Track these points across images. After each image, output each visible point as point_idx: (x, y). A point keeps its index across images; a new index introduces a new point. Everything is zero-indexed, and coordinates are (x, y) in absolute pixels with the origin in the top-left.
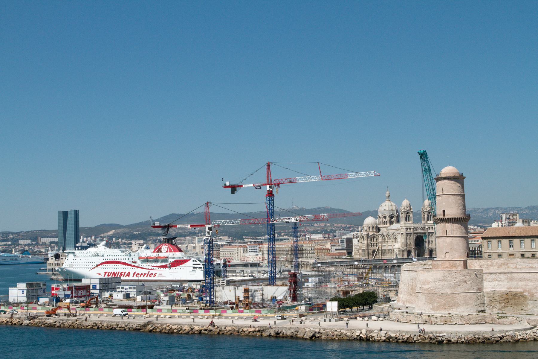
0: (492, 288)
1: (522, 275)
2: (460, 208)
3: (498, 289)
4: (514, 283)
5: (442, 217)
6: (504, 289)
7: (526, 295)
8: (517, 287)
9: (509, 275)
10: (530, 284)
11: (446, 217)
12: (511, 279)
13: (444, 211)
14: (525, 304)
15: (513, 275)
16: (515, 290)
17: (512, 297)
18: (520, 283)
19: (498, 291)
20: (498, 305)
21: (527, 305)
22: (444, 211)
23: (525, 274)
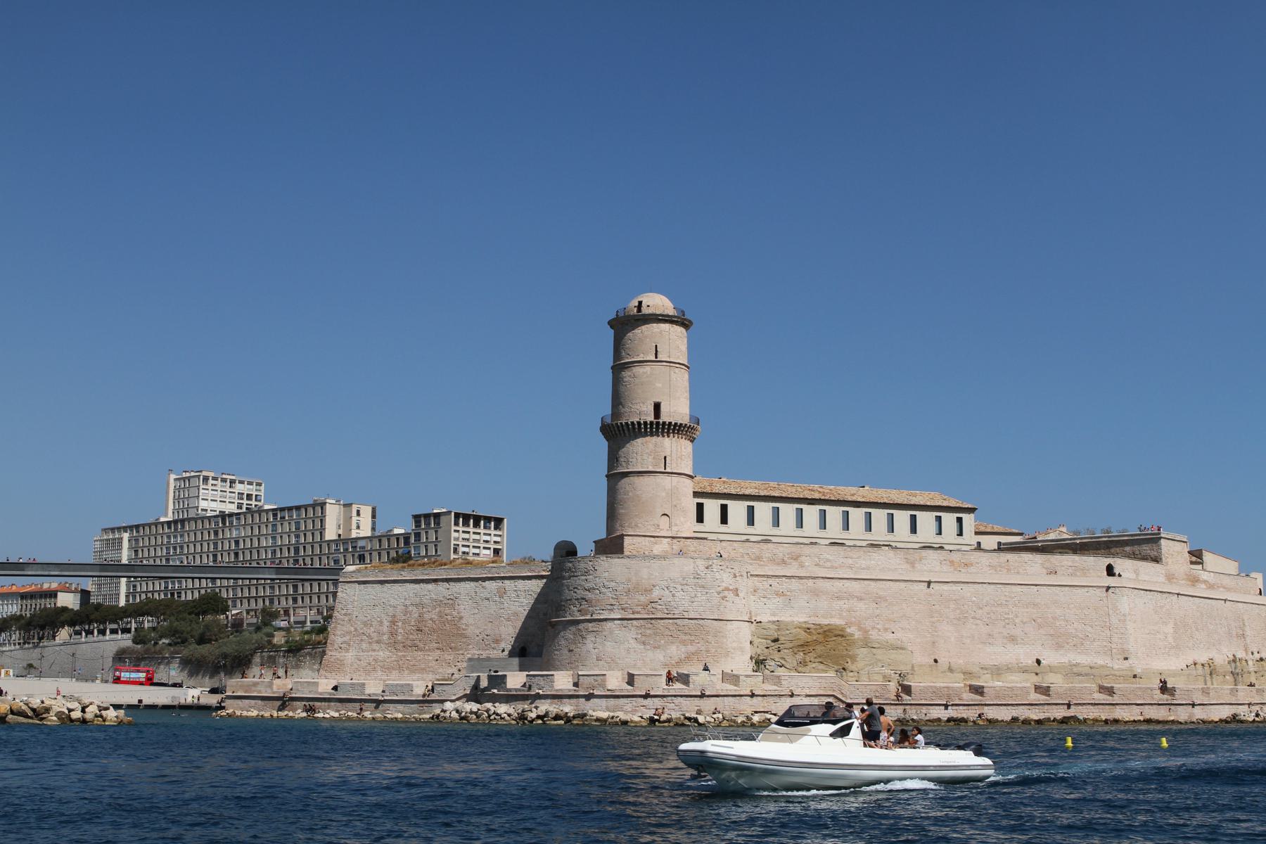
0: (774, 615)
1: (839, 584)
5: (651, 418)
6: (801, 618)
7: (852, 635)
10: (861, 605)
11: (665, 418)
12: (816, 593)
13: (657, 407)
15: (820, 583)
16: (825, 622)
17: (820, 638)
20: (789, 659)
21: (853, 658)
22: (657, 407)
23: (847, 583)
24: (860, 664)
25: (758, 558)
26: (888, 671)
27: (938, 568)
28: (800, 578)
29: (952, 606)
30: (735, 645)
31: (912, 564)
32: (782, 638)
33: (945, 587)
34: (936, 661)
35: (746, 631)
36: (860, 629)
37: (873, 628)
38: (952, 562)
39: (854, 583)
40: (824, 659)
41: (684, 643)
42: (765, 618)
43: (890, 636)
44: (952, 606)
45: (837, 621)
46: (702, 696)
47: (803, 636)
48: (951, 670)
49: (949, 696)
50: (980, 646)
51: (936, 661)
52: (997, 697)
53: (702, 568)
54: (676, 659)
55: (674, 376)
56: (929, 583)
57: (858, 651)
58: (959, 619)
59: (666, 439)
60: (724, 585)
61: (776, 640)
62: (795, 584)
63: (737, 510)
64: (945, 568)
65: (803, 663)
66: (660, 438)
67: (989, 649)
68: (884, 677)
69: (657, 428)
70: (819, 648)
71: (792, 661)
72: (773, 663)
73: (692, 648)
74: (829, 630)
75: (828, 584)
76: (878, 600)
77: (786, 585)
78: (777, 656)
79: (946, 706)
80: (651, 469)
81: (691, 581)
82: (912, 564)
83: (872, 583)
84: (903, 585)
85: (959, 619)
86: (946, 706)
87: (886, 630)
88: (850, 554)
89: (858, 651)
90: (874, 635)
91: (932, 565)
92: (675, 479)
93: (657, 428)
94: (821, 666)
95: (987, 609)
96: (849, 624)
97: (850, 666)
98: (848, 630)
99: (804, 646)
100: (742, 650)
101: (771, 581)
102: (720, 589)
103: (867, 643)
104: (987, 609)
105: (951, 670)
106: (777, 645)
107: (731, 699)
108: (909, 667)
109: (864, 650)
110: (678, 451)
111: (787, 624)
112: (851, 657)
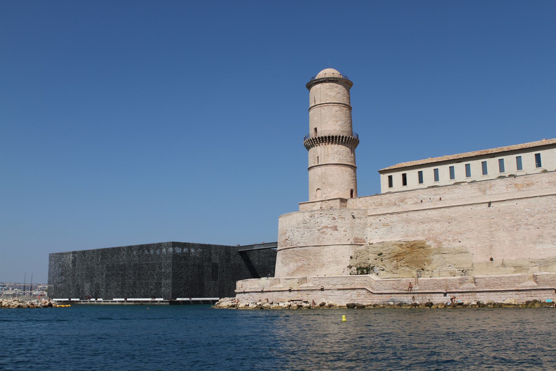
0: (381, 238)
1: (423, 213)
2: (340, 123)
3: (387, 239)
4: (412, 227)
7: (429, 246)
8: (414, 233)
9: (404, 215)
10: (437, 226)
12: (408, 221)
14: (427, 261)
18: (421, 227)
19: (389, 243)
21: (429, 262)
23: (429, 212)
24: (434, 265)
25: (381, 205)
26: (452, 269)
27: (505, 191)
28: (398, 213)
29: (508, 218)
30: (330, 260)
31: (484, 192)
32: (384, 253)
33: (503, 204)
34: (492, 259)
35: (349, 251)
36: (436, 241)
37: (445, 240)
38: (516, 185)
39: (434, 211)
40: (409, 264)
41: (296, 261)
42: (374, 241)
43: (456, 245)
44: (508, 218)
45: (420, 238)
46: (262, 292)
47: (398, 249)
48: (503, 265)
49: (447, 287)
50: (531, 245)
51: (492, 259)
52: (486, 286)
53: (307, 217)
54: (292, 271)
55: (323, 111)
56: (490, 203)
57: (432, 257)
58: (513, 227)
59: (319, 147)
60: (323, 225)
61: (380, 254)
62: (395, 218)
63: (412, 175)
64: (510, 190)
65: (397, 267)
66: (316, 147)
67: (539, 247)
68: (451, 273)
69: (333, 140)
70: (408, 257)
71: (389, 266)
72: (378, 269)
73: (300, 264)
74: (414, 245)
75: (416, 214)
76: (450, 221)
77: (389, 218)
78: (380, 264)
79: (445, 294)
80: (313, 165)
81: (302, 225)
82: (484, 192)
83: (447, 210)
84: (469, 208)
85: (513, 227)
86: (445, 294)
87: (454, 240)
88: (439, 192)
89: (432, 257)
90: (445, 245)
91: (501, 190)
92: (323, 168)
93: (333, 140)
94: (408, 269)
95: (539, 216)
96: (428, 239)
97: (427, 267)
98: (427, 243)
99: (397, 256)
100: (338, 263)
101: (380, 218)
102: (320, 228)
103: (440, 251)
104: (539, 216)
105: (503, 265)
106: (381, 257)
107: (277, 293)
108: (470, 265)
109: (437, 256)
110: (336, 153)
111: (388, 243)
112: (427, 261)
